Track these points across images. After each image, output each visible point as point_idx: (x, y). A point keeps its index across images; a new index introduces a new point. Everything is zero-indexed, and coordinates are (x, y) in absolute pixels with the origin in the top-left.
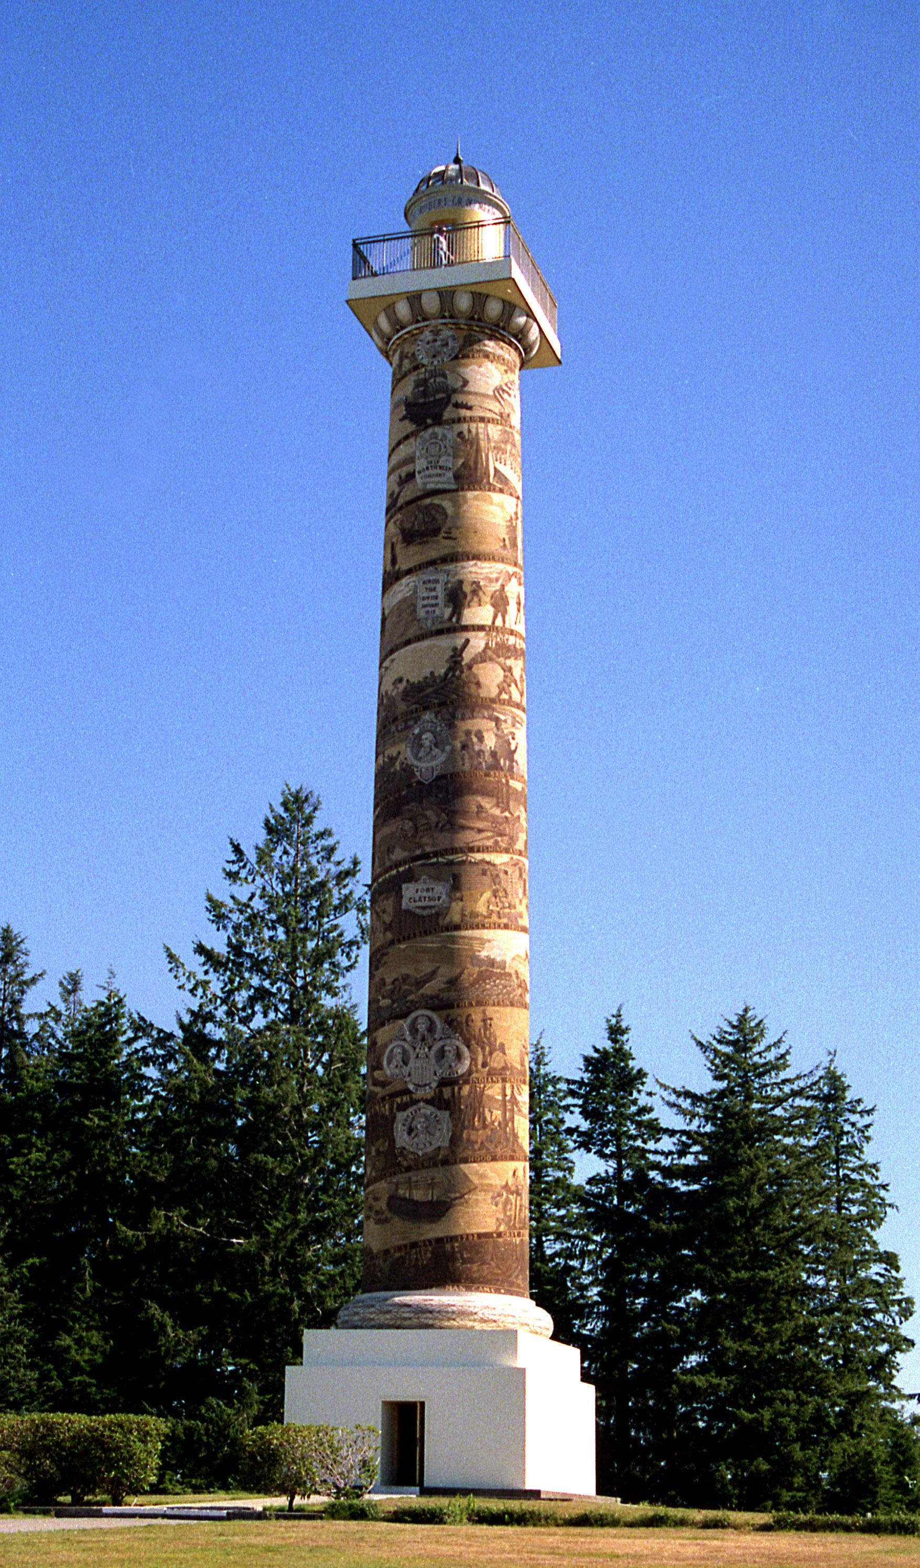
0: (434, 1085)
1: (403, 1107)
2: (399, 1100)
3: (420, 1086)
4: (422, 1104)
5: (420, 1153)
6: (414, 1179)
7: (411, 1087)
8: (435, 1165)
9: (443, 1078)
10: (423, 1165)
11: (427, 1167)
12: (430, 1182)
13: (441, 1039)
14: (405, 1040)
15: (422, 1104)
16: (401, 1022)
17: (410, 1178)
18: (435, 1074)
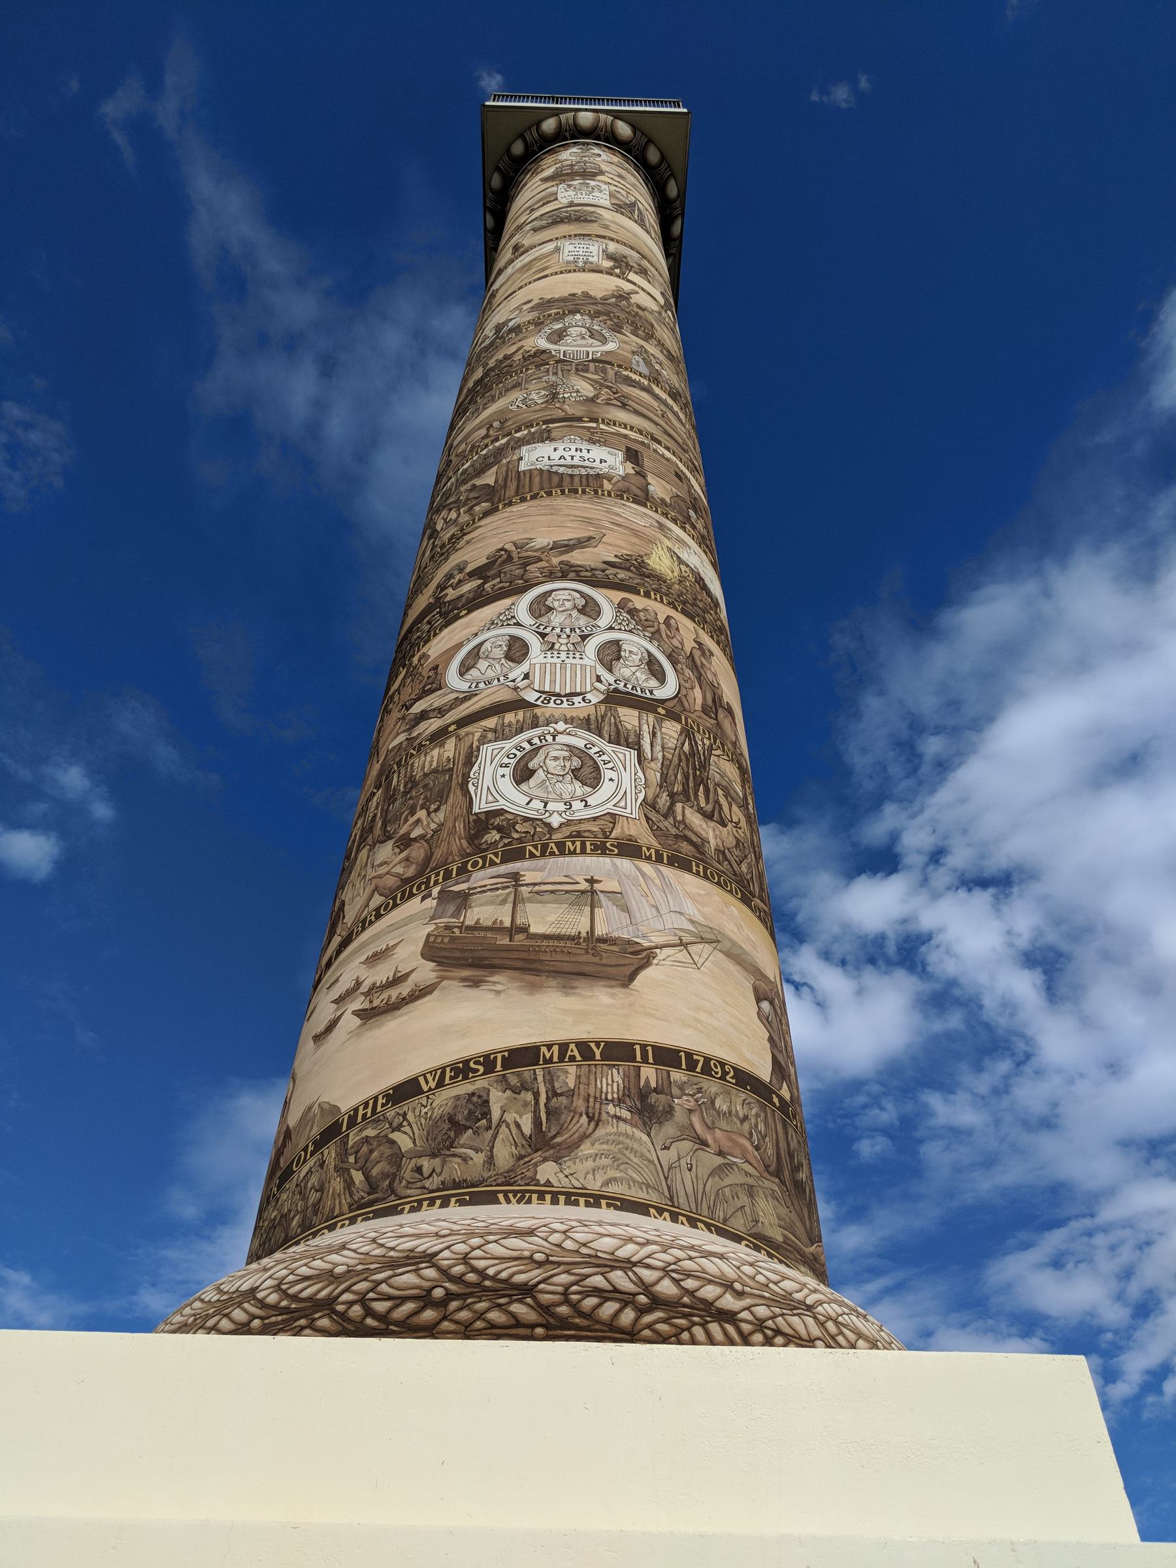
0: (595, 698)
1: (500, 734)
2: (491, 722)
3: (559, 695)
4: (561, 726)
5: (555, 821)
6: (529, 877)
7: (531, 696)
8: (601, 849)
9: (616, 690)
10: (561, 846)
11: (573, 853)
12: (584, 886)
13: (611, 628)
14: (518, 624)
15: (561, 726)
16: (507, 602)
17: (515, 877)
18: (600, 682)
